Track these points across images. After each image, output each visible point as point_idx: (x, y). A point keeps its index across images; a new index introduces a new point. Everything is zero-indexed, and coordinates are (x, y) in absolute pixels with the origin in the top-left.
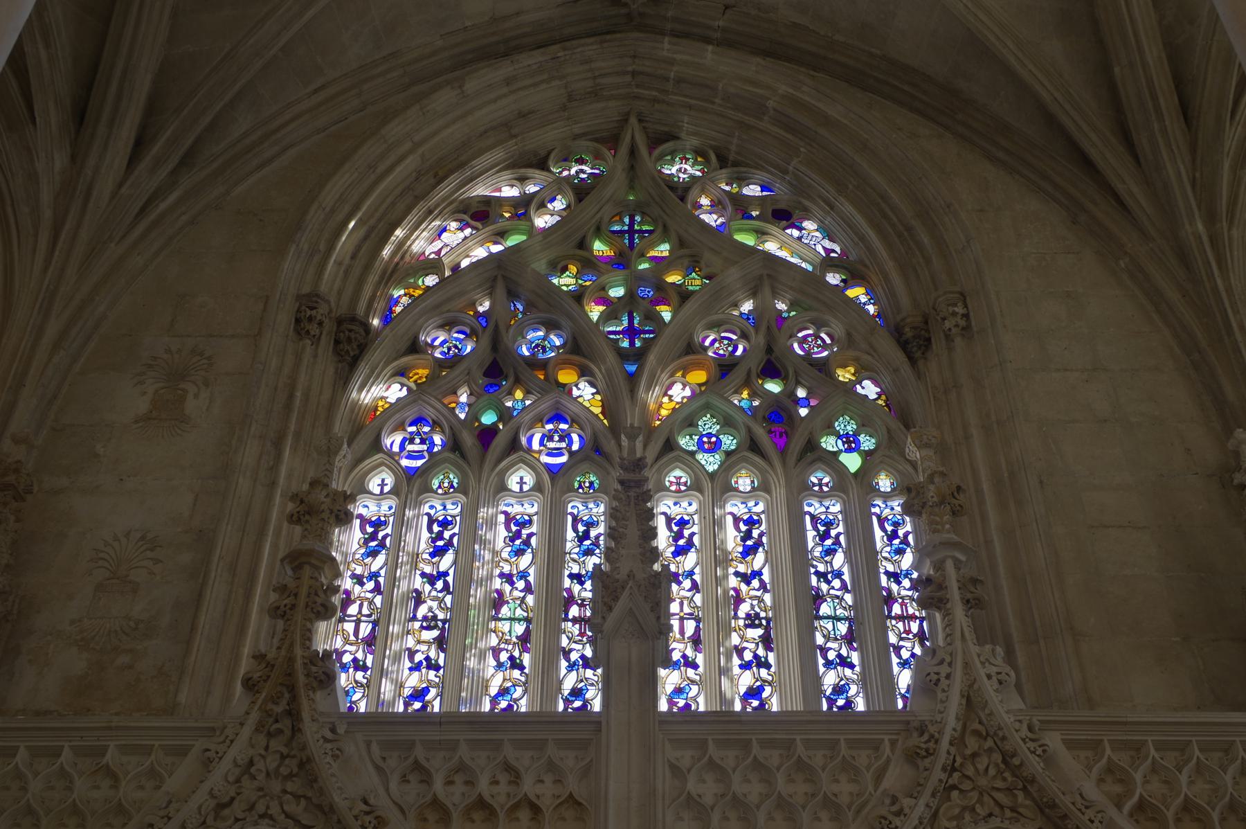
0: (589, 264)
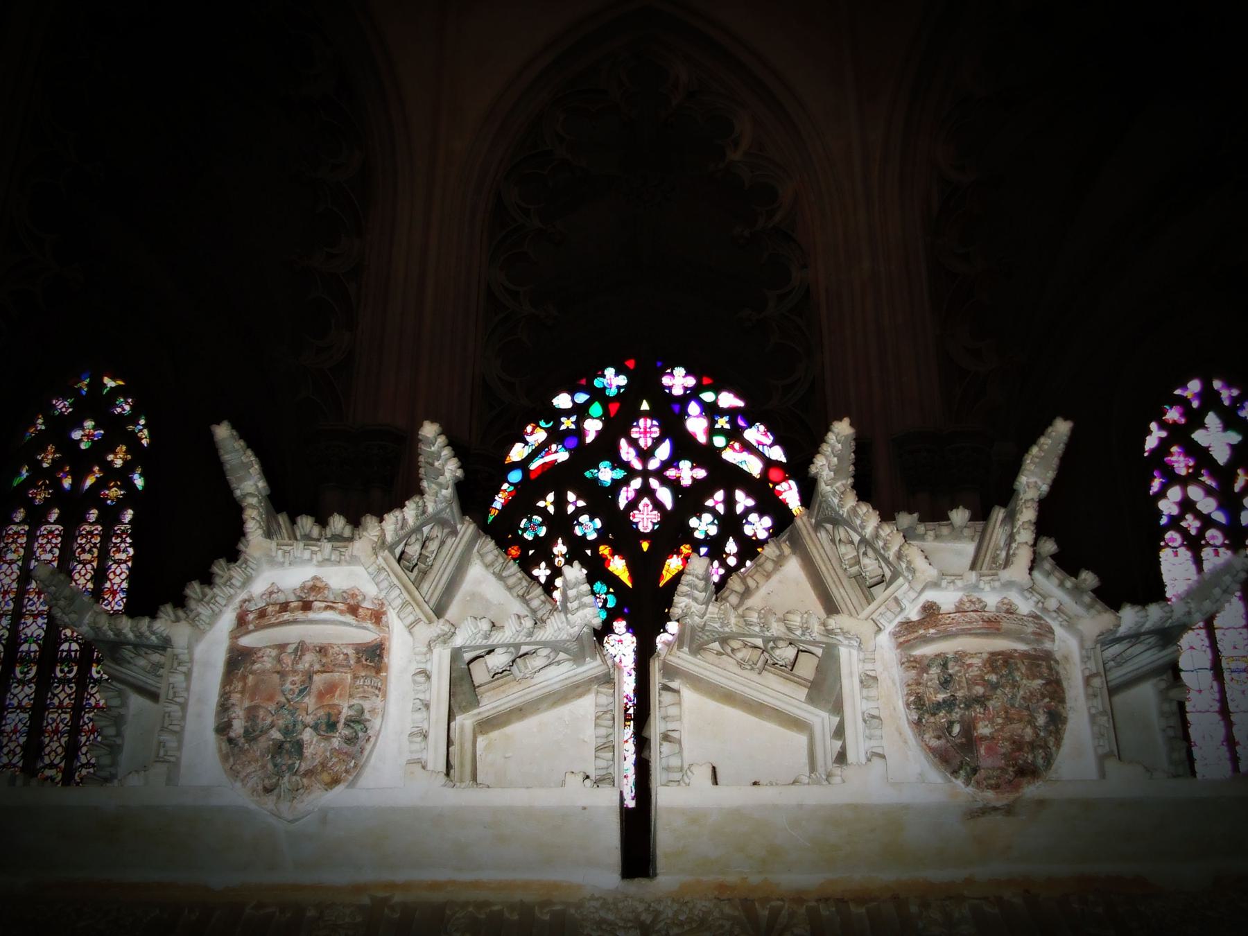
0: (618, 463)
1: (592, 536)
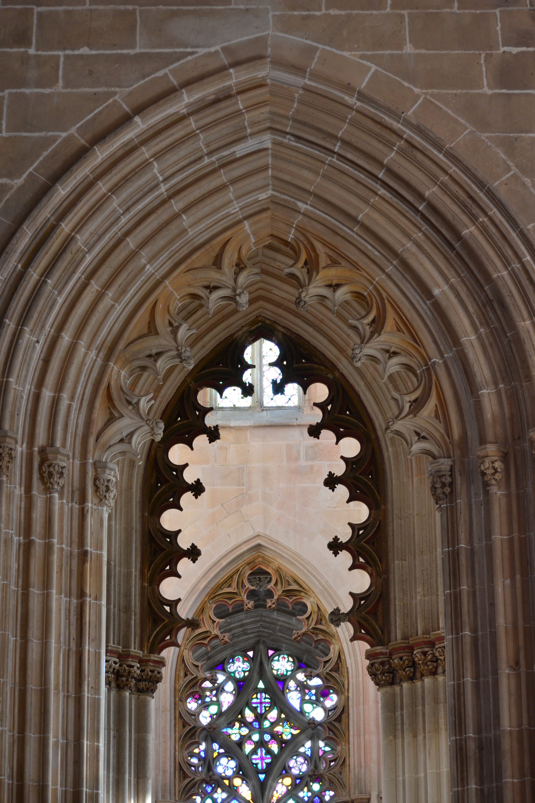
0: (244, 723)
1: (229, 773)
